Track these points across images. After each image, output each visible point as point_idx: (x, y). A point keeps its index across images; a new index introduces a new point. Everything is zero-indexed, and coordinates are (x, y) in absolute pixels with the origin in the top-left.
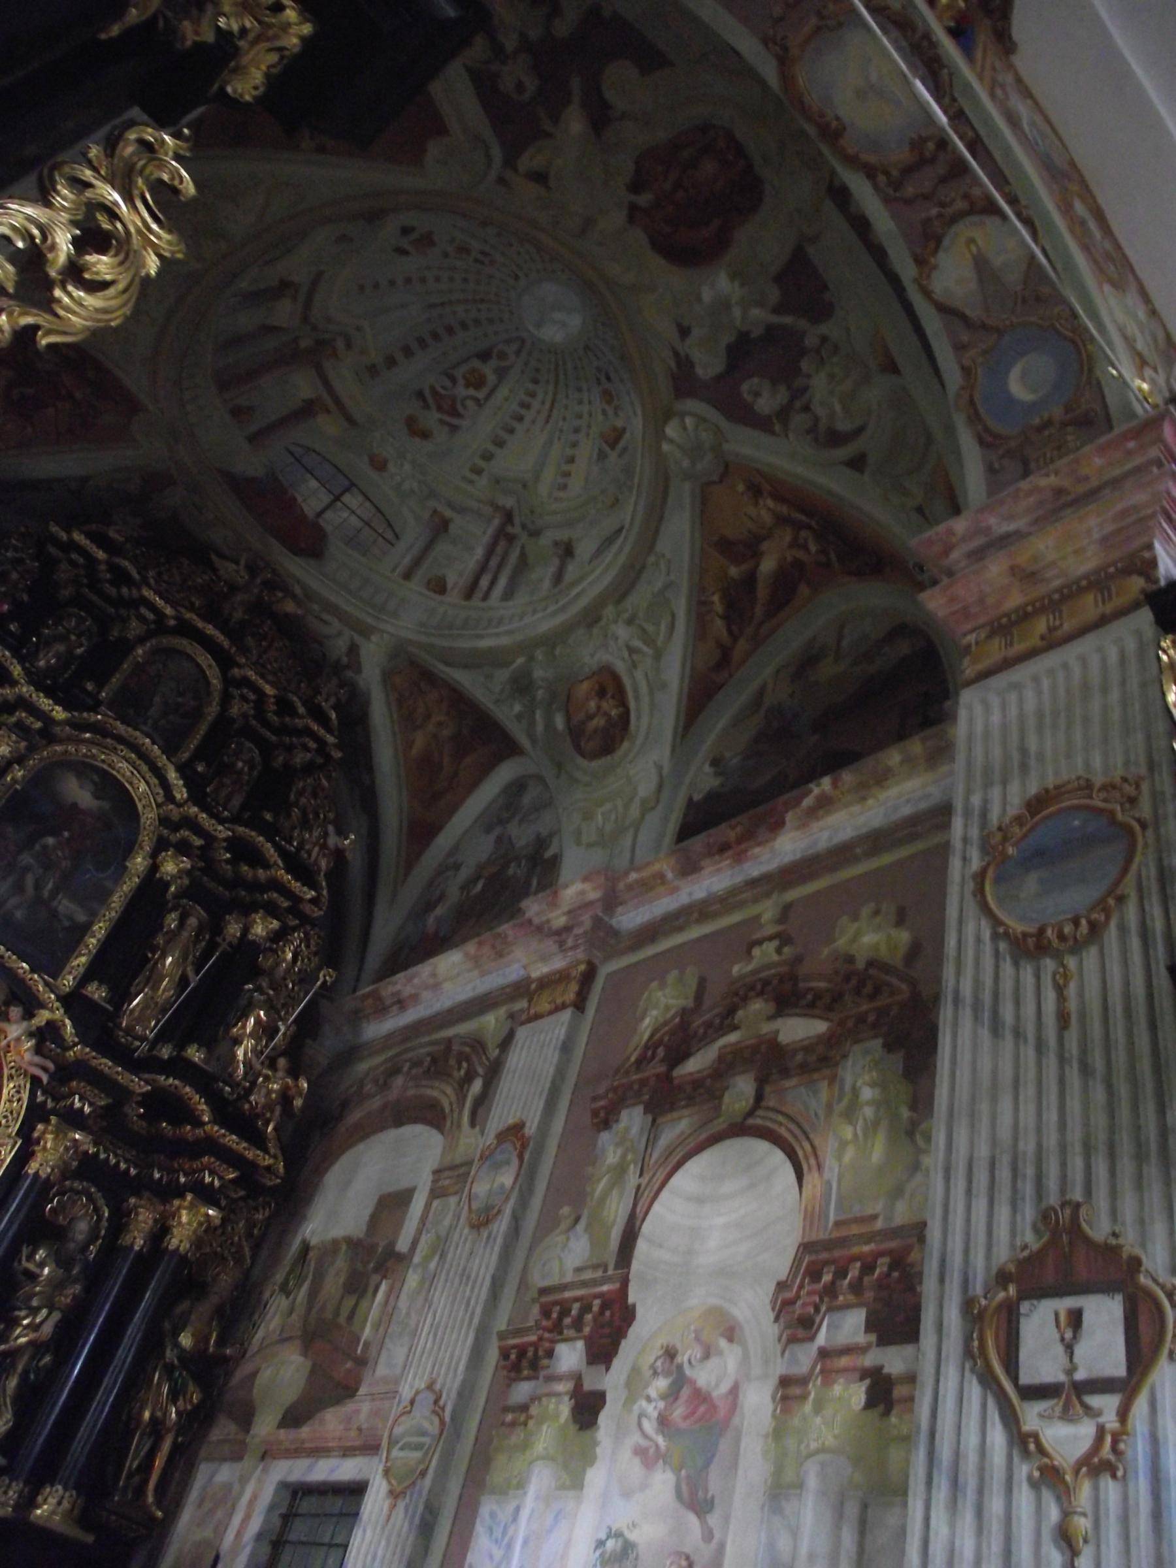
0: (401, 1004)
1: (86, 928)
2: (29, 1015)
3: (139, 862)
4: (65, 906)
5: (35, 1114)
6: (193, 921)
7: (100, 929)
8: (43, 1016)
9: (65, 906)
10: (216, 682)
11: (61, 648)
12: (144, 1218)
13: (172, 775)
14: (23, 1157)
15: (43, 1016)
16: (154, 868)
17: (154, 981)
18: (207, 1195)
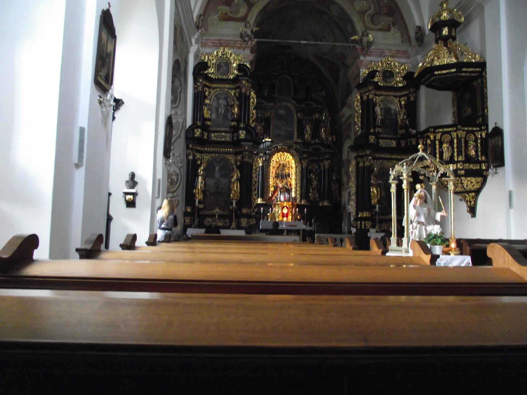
0: (343, 116)
1: (293, 131)
2: (292, 148)
3: (295, 116)
4: (289, 129)
5: (300, 160)
6: (307, 120)
7: (295, 130)
8: (294, 147)
9: (289, 129)
10: (290, 78)
11: (266, 90)
12: (322, 164)
13: (292, 101)
14: (302, 166)
15: (294, 147)
16: (297, 117)
17: (307, 131)
18: (327, 159)
